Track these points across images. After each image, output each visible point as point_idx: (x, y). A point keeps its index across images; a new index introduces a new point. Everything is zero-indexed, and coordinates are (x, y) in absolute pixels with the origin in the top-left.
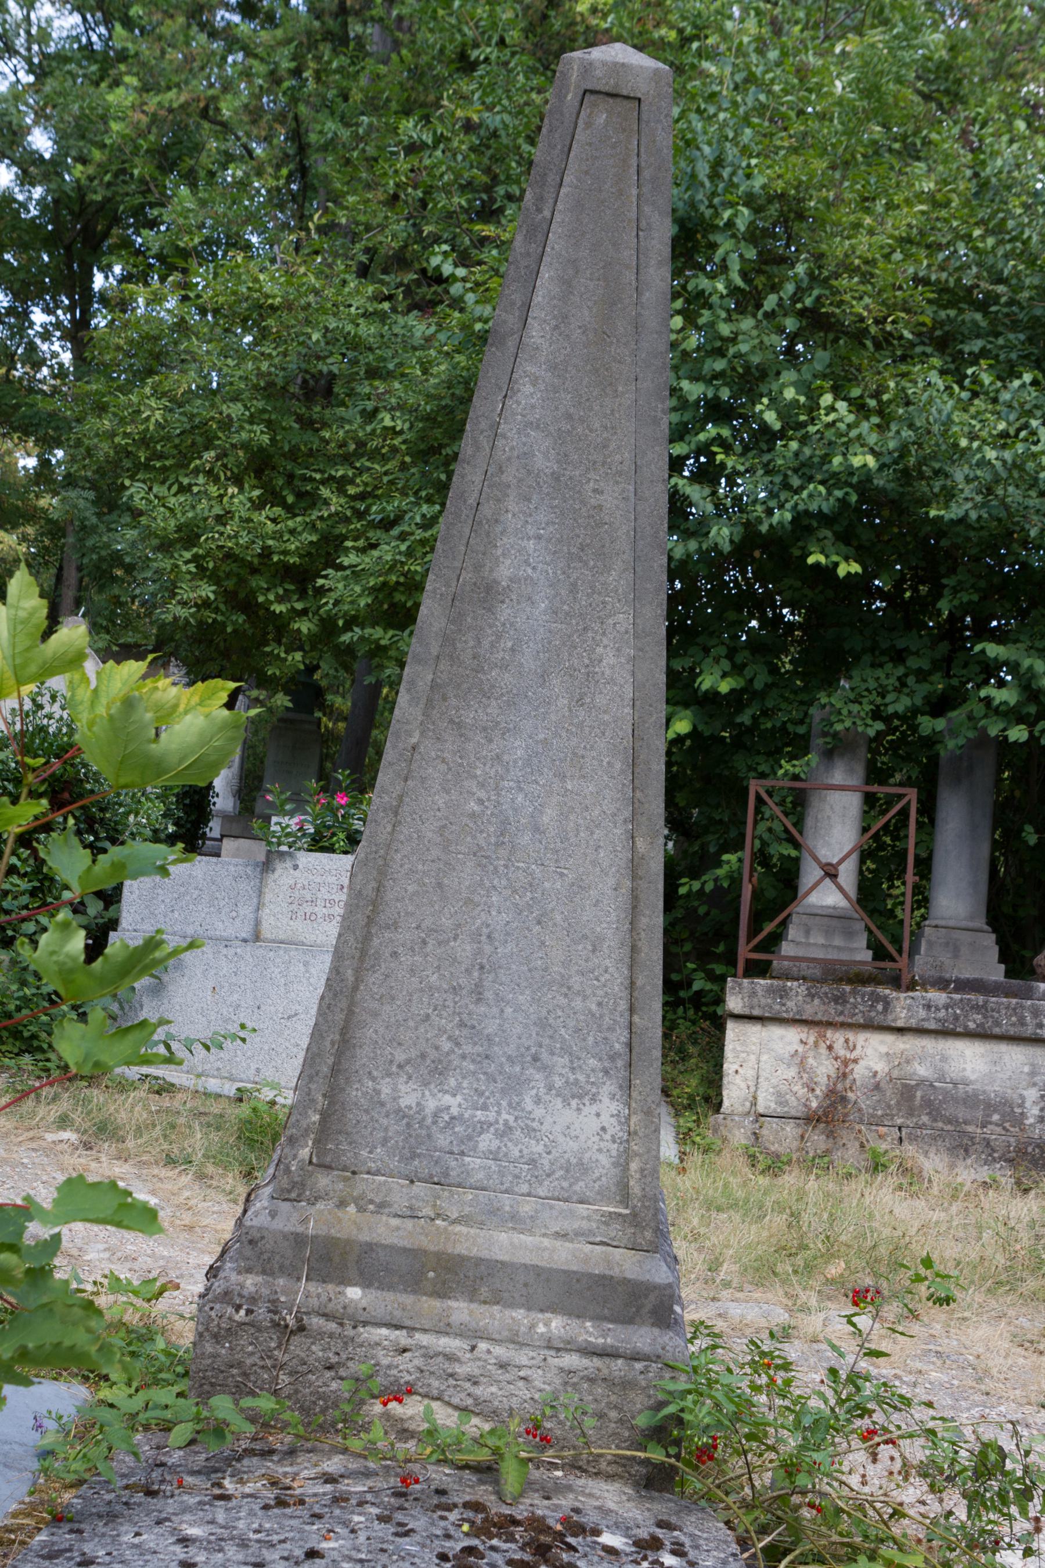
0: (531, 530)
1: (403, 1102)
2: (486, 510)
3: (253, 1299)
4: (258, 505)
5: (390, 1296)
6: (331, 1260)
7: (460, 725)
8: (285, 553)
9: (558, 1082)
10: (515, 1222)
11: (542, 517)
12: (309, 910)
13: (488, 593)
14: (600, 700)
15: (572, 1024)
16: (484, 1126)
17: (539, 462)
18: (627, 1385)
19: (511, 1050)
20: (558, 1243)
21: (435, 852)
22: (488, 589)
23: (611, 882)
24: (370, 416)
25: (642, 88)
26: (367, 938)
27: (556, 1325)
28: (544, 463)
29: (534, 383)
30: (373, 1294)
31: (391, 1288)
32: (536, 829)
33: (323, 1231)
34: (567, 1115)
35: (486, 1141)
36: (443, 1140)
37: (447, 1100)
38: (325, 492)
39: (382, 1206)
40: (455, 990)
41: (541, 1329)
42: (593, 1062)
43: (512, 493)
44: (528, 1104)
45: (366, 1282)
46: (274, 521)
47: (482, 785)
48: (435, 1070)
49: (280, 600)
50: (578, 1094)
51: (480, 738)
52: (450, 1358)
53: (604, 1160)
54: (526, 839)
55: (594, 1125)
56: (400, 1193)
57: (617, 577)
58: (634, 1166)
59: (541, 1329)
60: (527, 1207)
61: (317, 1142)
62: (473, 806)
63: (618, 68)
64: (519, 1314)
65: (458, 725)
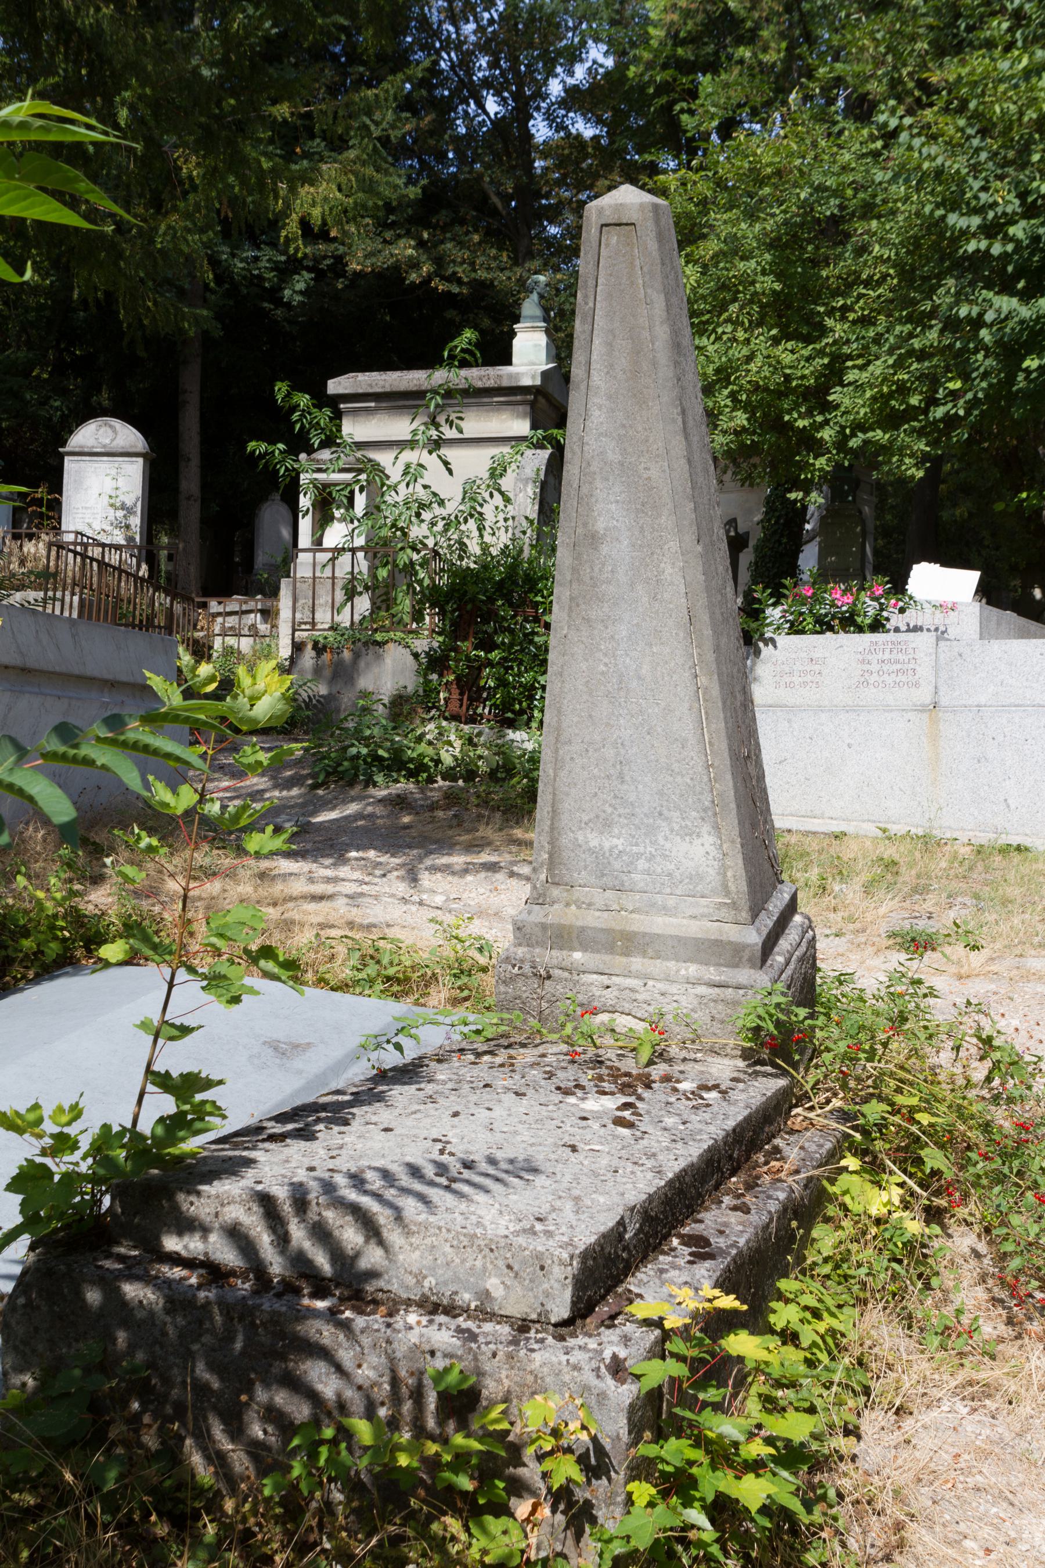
0: (612, 498)
1: (592, 844)
2: (585, 490)
3: (522, 961)
4: (776, 341)
5: (598, 956)
6: (562, 937)
7: (588, 620)
8: (803, 377)
9: (676, 827)
10: (666, 910)
11: (617, 489)
13: (594, 539)
16: (639, 855)
18: (736, 1003)
19: (645, 810)
20: (692, 922)
21: (585, 697)
22: (593, 537)
23: (687, 705)
24: (862, 250)
25: (634, 216)
26: (557, 751)
27: (692, 970)
28: (613, 456)
29: (600, 408)
30: (588, 955)
31: (598, 951)
32: (639, 678)
33: (556, 921)
35: (642, 864)
36: (617, 865)
37: (615, 841)
38: (829, 322)
39: (590, 905)
40: (608, 777)
41: (683, 972)
42: (694, 814)
43: (598, 477)
44: (661, 841)
45: (584, 949)
46: (792, 352)
48: (606, 825)
49: (801, 416)
50: (689, 833)
51: (600, 626)
52: (632, 990)
54: (634, 684)
55: (701, 851)
56: (599, 898)
57: (666, 520)
58: (729, 874)
59: (683, 972)
60: (671, 902)
61: (549, 870)
62: (602, 668)
63: (619, 207)
64: (672, 964)
65: (588, 620)
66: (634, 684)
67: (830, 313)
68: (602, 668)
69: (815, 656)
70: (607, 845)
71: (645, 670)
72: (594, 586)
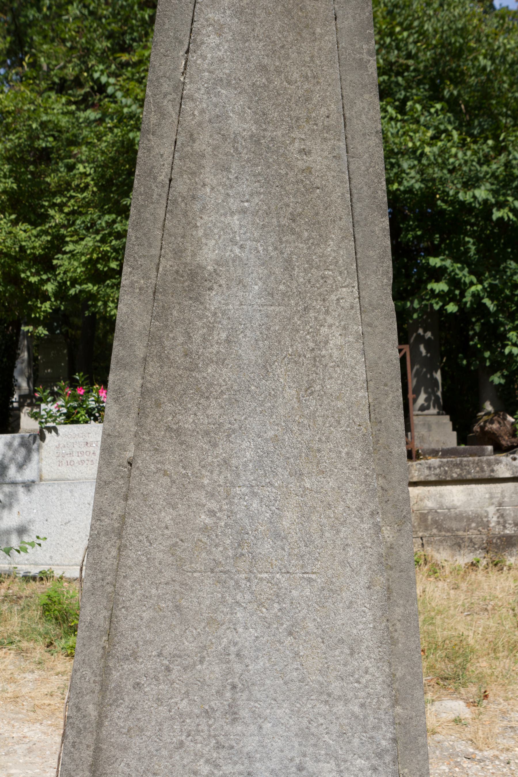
0: (234, 204)
2: (181, 186)
4: (15, 223)
7: (178, 432)
8: (34, 248)
11: (244, 188)
12: (69, 459)
13: (194, 281)
14: (331, 386)
15: (334, 729)
17: (235, 124)
21: (168, 574)
22: (193, 276)
23: (363, 580)
24: (71, 168)
26: (106, 671)
28: (241, 125)
32: (277, 535)
38: (51, 212)
42: (360, 762)
43: (208, 163)
46: (25, 231)
47: (211, 495)
49: (33, 275)
51: (203, 443)
54: (266, 547)
57: (336, 248)
62: (204, 519)
66: (266, 547)
67: (53, 205)
69: (90, 440)
71: (288, 520)
72: (193, 368)
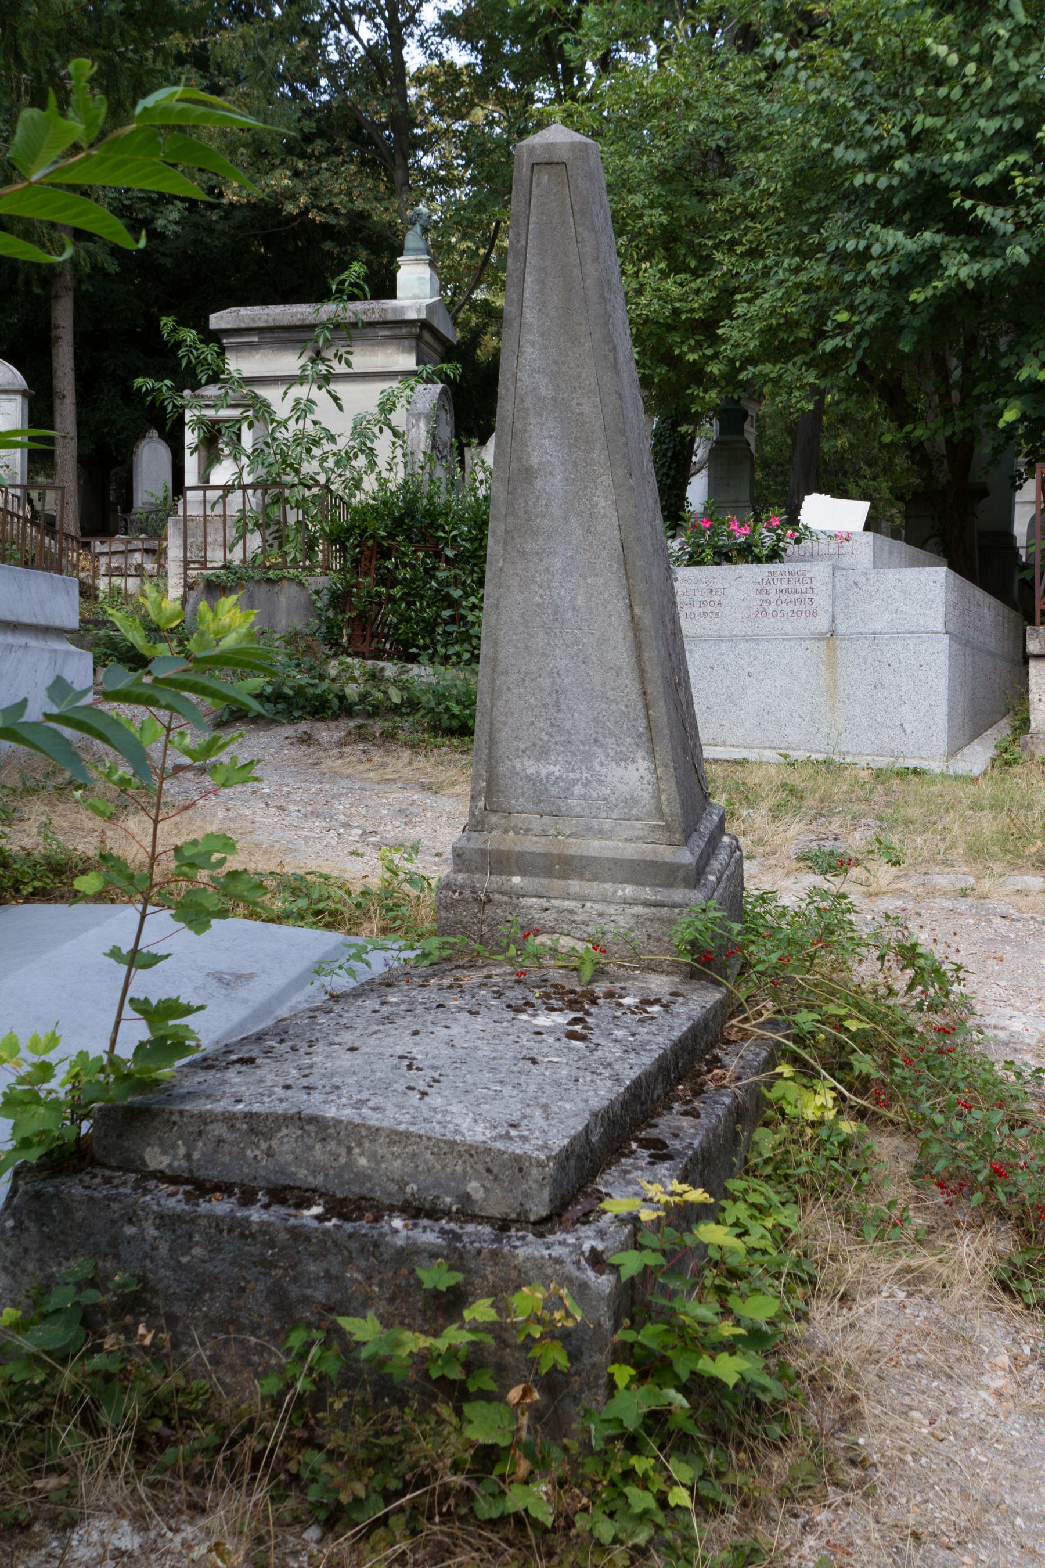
2: (518, 425)
3: (462, 887)
4: (664, 275)
5: (536, 880)
6: (502, 862)
7: (523, 553)
8: (692, 310)
9: (611, 753)
10: (602, 834)
11: (549, 425)
14: (600, 528)
17: (543, 392)
18: (671, 922)
19: (581, 737)
21: (521, 629)
24: (748, 183)
25: (565, 156)
26: (494, 681)
27: (629, 890)
30: (527, 879)
31: (536, 875)
32: (574, 609)
33: (495, 847)
34: (619, 772)
35: (578, 790)
36: (554, 791)
37: (552, 768)
38: (718, 256)
39: (527, 830)
40: (545, 706)
44: (597, 767)
45: (523, 873)
46: (681, 285)
48: (543, 753)
49: (692, 349)
50: (623, 759)
52: (571, 912)
53: (646, 795)
54: (569, 615)
55: (636, 775)
56: (537, 823)
57: (599, 454)
58: (663, 797)
60: (607, 825)
62: (538, 599)
63: (550, 147)
64: (608, 886)
65: (523, 553)
66: (569, 615)
68: (538, 599)
69: (714, 586)
70: (544, 772)
71: (580, 601)
72: (529, 519)
